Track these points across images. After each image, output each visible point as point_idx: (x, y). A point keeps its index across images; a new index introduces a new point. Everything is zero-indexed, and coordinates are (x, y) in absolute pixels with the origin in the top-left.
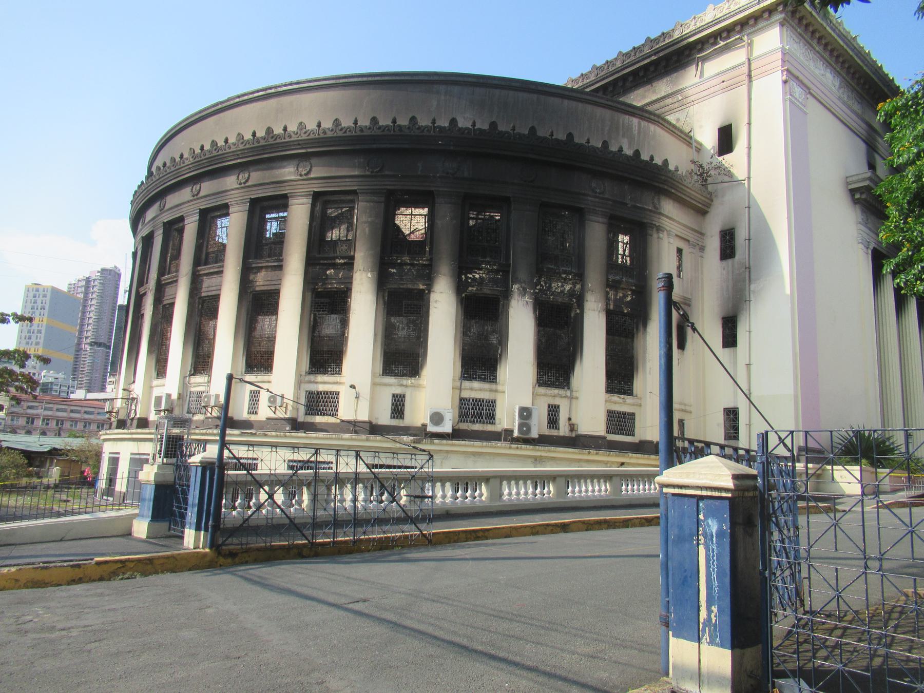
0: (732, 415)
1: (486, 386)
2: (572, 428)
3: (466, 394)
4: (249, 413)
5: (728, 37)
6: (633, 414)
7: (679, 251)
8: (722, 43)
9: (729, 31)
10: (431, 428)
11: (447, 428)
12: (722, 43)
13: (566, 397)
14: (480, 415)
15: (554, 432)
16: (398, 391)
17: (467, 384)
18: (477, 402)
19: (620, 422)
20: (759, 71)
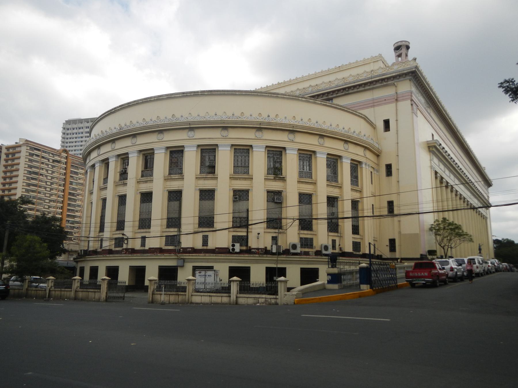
0: (392, 242)
1: (309, 232)
2: (340, 249)
3: (302, 236)
4: (203, 246)
5: (387, 81)
6: (360, 243)
7: (371, 172)
8: (385, 83)
9: (388, 79)
10: (292, 251)
11: (298, 250)
12: (385, 83)
13: (338, 236)
14: (307, 245)
15: (334, 251)
16: (274, 235)
17: (302, 232)
18: (306, 239)
19: (356, 246)
20: (401, 98)
